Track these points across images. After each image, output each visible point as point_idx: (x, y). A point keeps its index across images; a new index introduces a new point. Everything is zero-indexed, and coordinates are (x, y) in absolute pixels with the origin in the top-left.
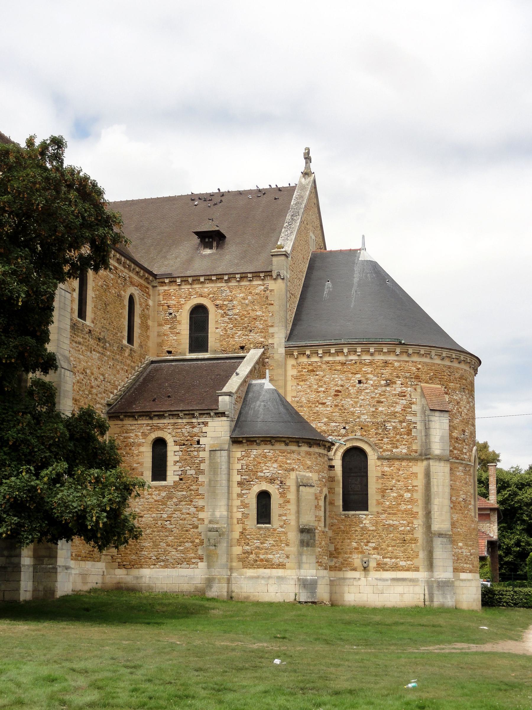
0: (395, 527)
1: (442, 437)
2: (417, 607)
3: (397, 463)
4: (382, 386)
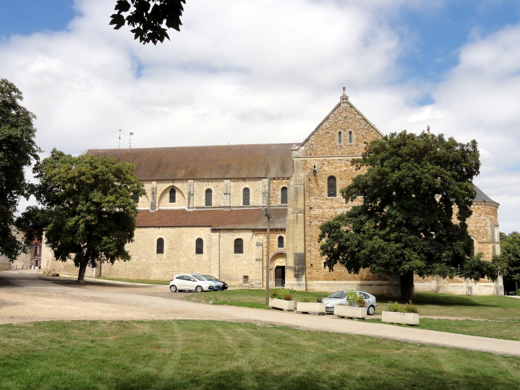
2: (492, 295)
3: (484, 244)
4: (478, 216)
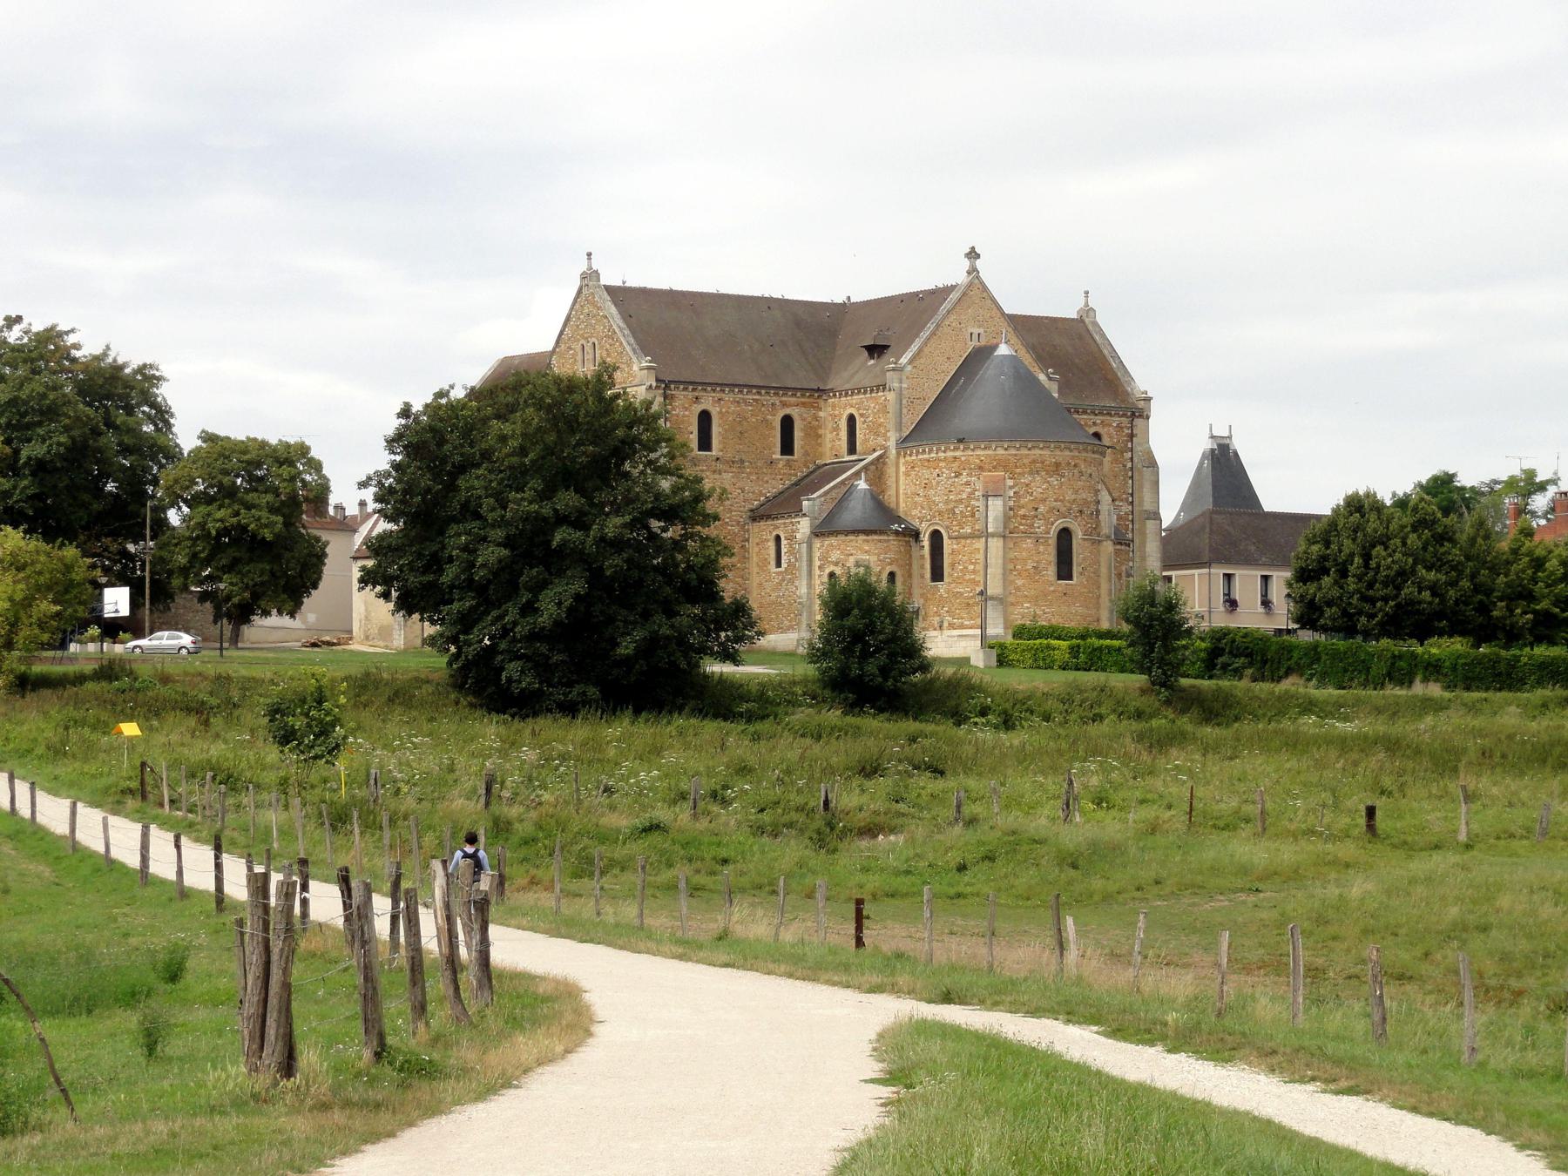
0: (962, 594)
1: (996, 519)
3: (963, 541)
4: (951, 478)
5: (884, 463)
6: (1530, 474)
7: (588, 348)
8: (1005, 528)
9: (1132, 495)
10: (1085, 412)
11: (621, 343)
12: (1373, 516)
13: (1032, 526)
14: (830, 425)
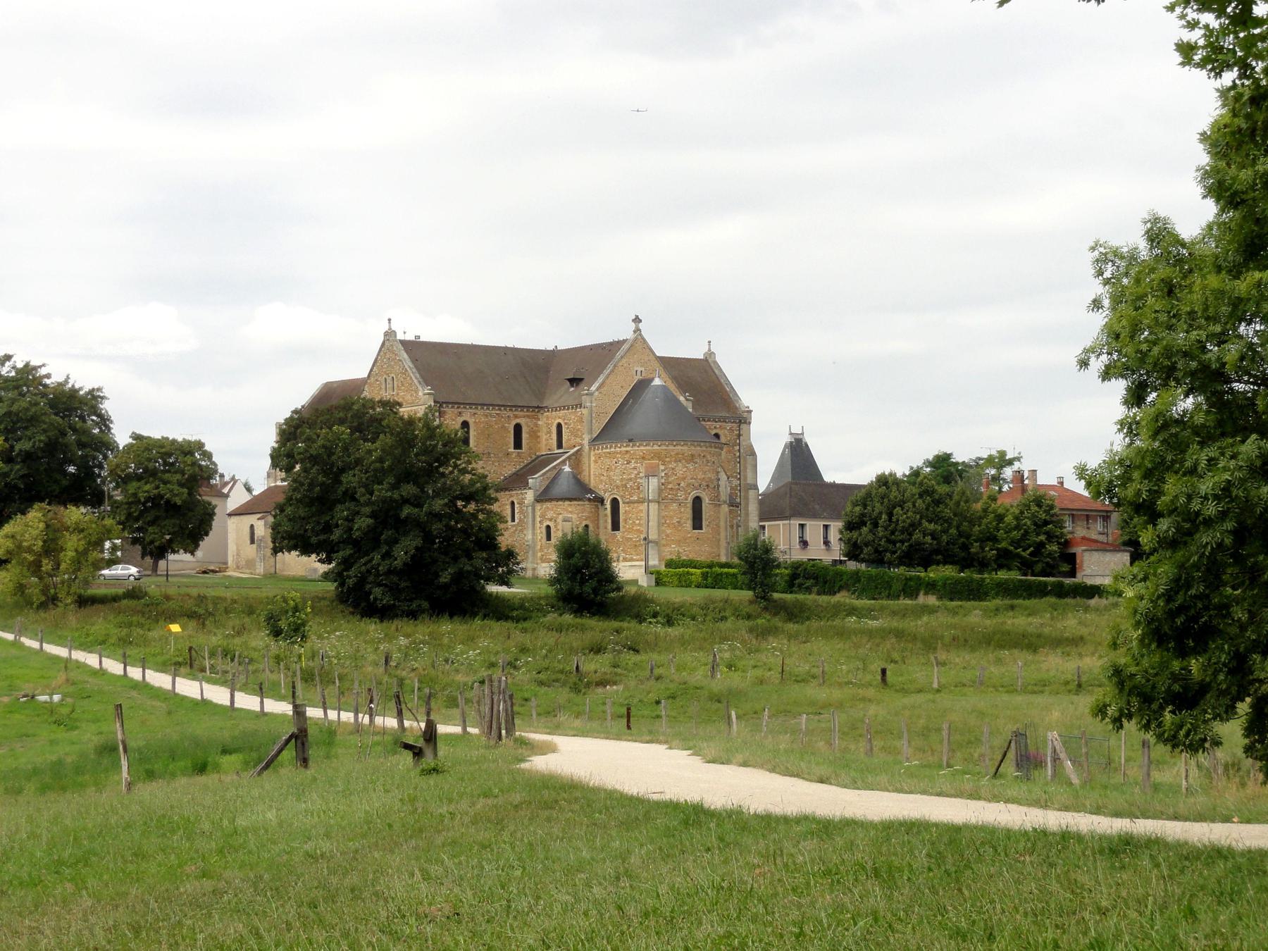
5: (581, 455)
6: (1002, 454)
7: (389, 380)
8: (659, 496)
9: (740, 474)
10: (709, 420)
11: (411, 378)
12: (894, 488)
13: (676, 495)
14: (545, 430)
